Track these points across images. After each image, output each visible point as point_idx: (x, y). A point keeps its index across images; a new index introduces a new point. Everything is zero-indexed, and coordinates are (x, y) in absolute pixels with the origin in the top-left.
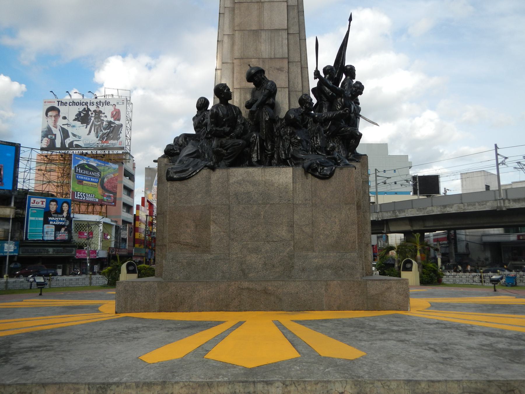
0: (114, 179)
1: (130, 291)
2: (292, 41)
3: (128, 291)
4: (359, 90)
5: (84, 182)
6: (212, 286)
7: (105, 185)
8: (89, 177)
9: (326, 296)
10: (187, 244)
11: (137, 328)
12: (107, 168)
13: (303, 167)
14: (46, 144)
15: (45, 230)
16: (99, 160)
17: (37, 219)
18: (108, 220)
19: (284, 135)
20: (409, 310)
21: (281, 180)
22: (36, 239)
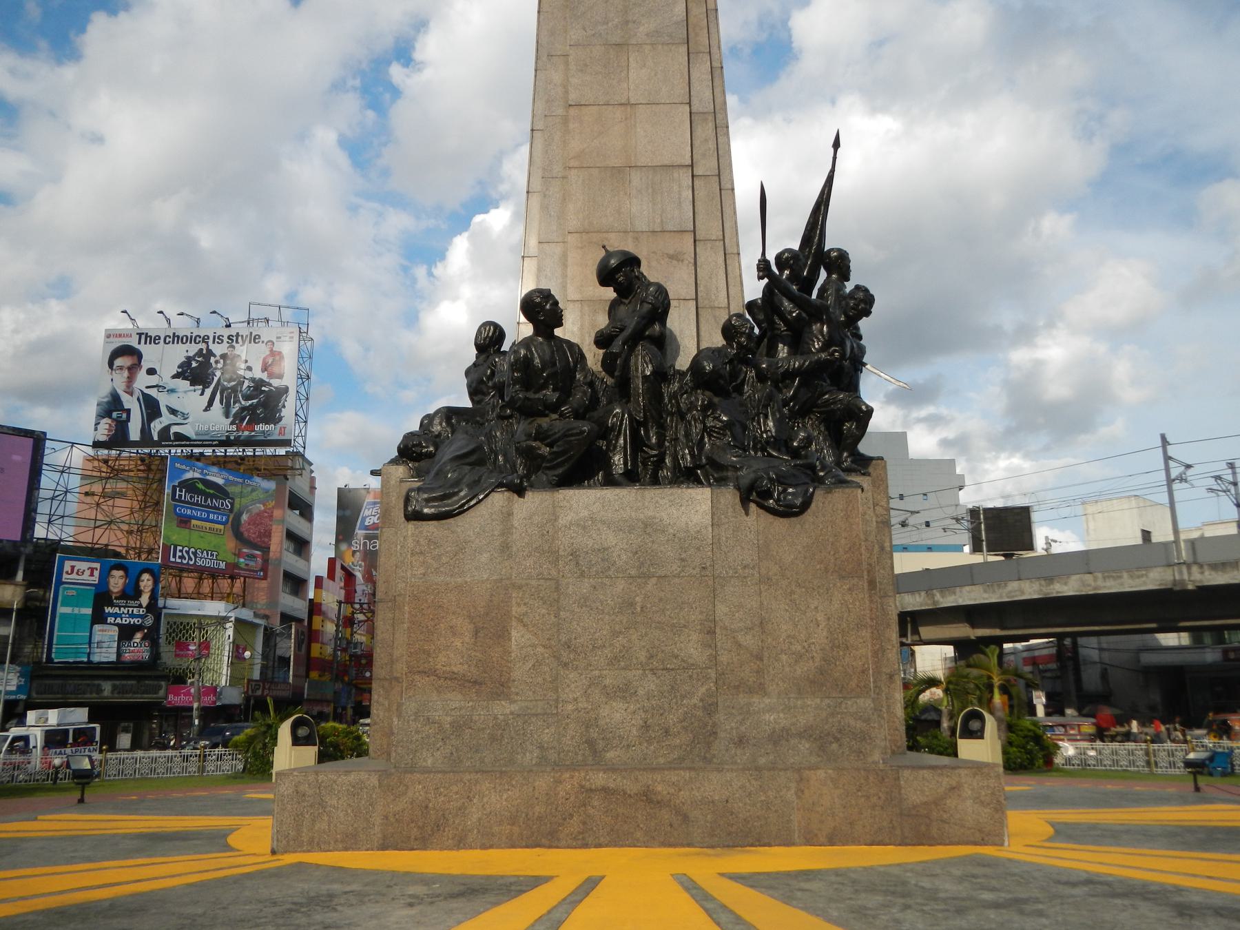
0: (266, 514)
1: (309, 796)
2: (700, 194)
3: (304, 795)
4: (863, 306)
5: (194, 522)
7: (242, 529)
8: (204, 511)
9: (798, 809)
10: (452, 677)
11: (331, 896)
12: (249, 489)
13: (738, 488)
14: (106, 432)
15: (96, 638)
16: (230, 471)
17: (76, 610)
18: (246, 614)
19: (689, 410)
20: (1006, 843)
21: (684, 519)
22: (71, 660)
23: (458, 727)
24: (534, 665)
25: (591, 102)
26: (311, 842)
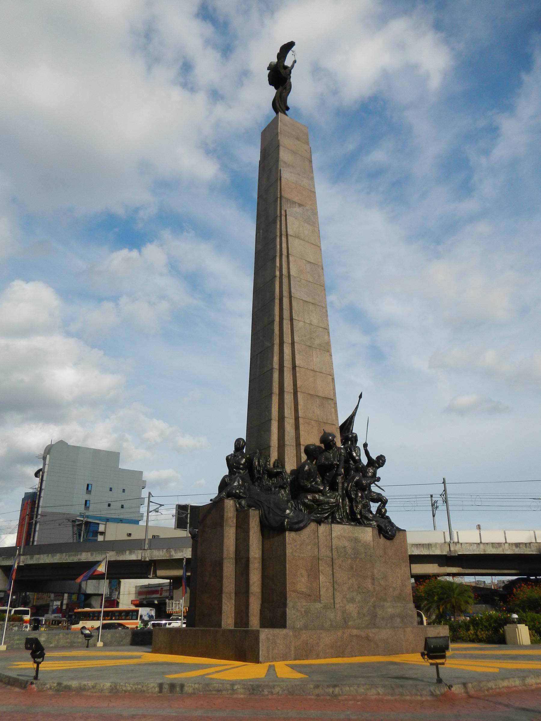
6: (332, 633)
10: (302, 593)
23: (307, 612)
24: (326, 590)
25: (302, 366)
26: (272, 658)
